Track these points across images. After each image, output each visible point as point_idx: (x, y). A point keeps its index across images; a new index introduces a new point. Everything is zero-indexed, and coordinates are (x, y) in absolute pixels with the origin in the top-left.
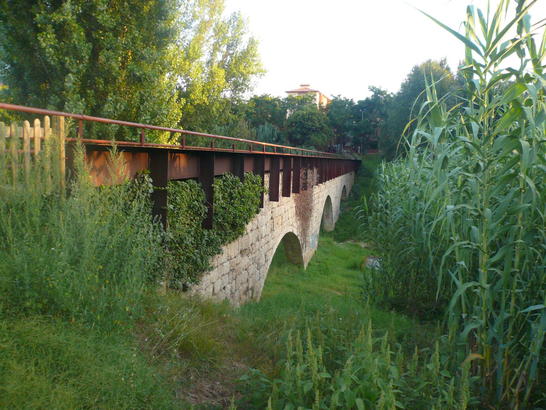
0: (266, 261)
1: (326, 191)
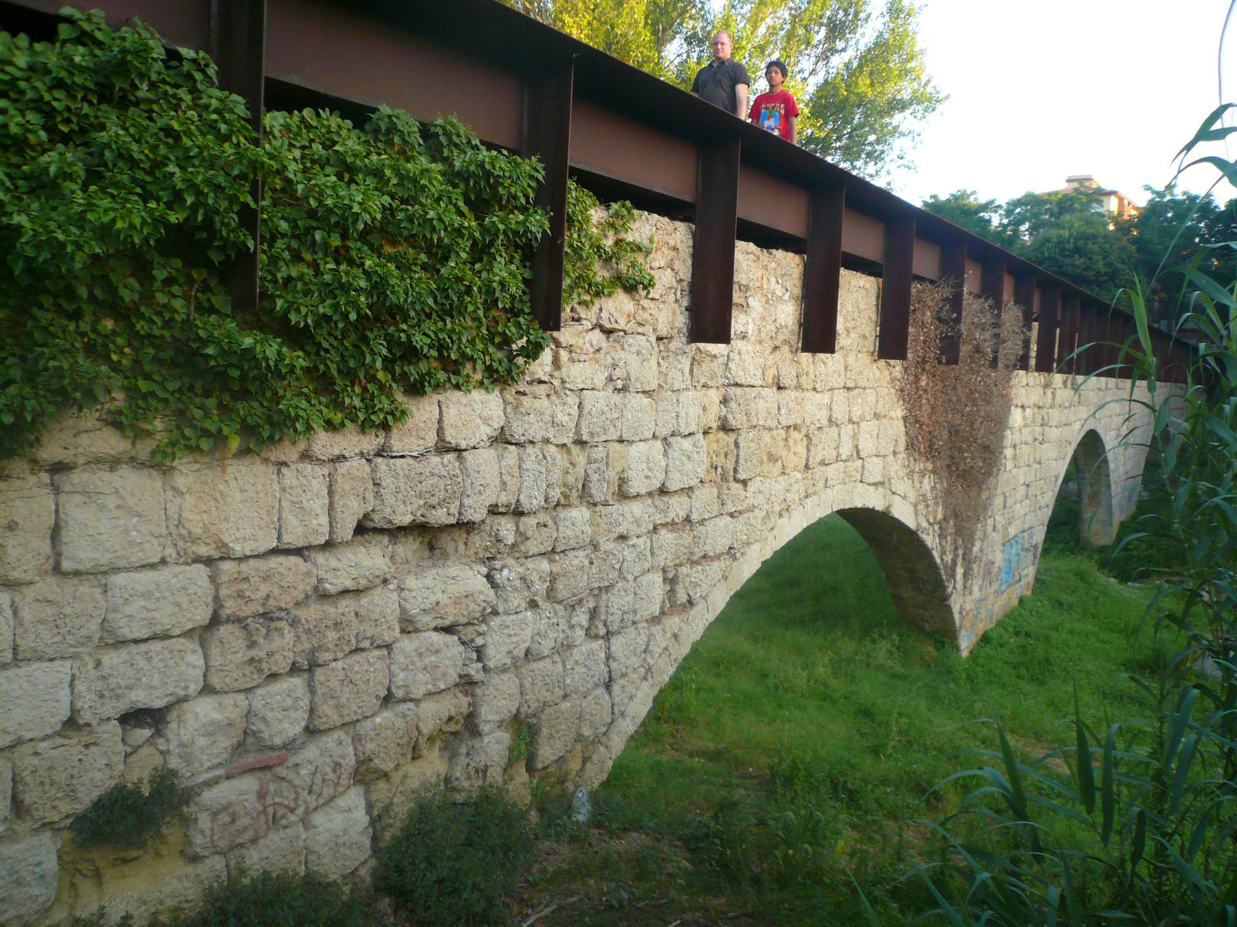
0: (676, 604)
1: (1084, 412)
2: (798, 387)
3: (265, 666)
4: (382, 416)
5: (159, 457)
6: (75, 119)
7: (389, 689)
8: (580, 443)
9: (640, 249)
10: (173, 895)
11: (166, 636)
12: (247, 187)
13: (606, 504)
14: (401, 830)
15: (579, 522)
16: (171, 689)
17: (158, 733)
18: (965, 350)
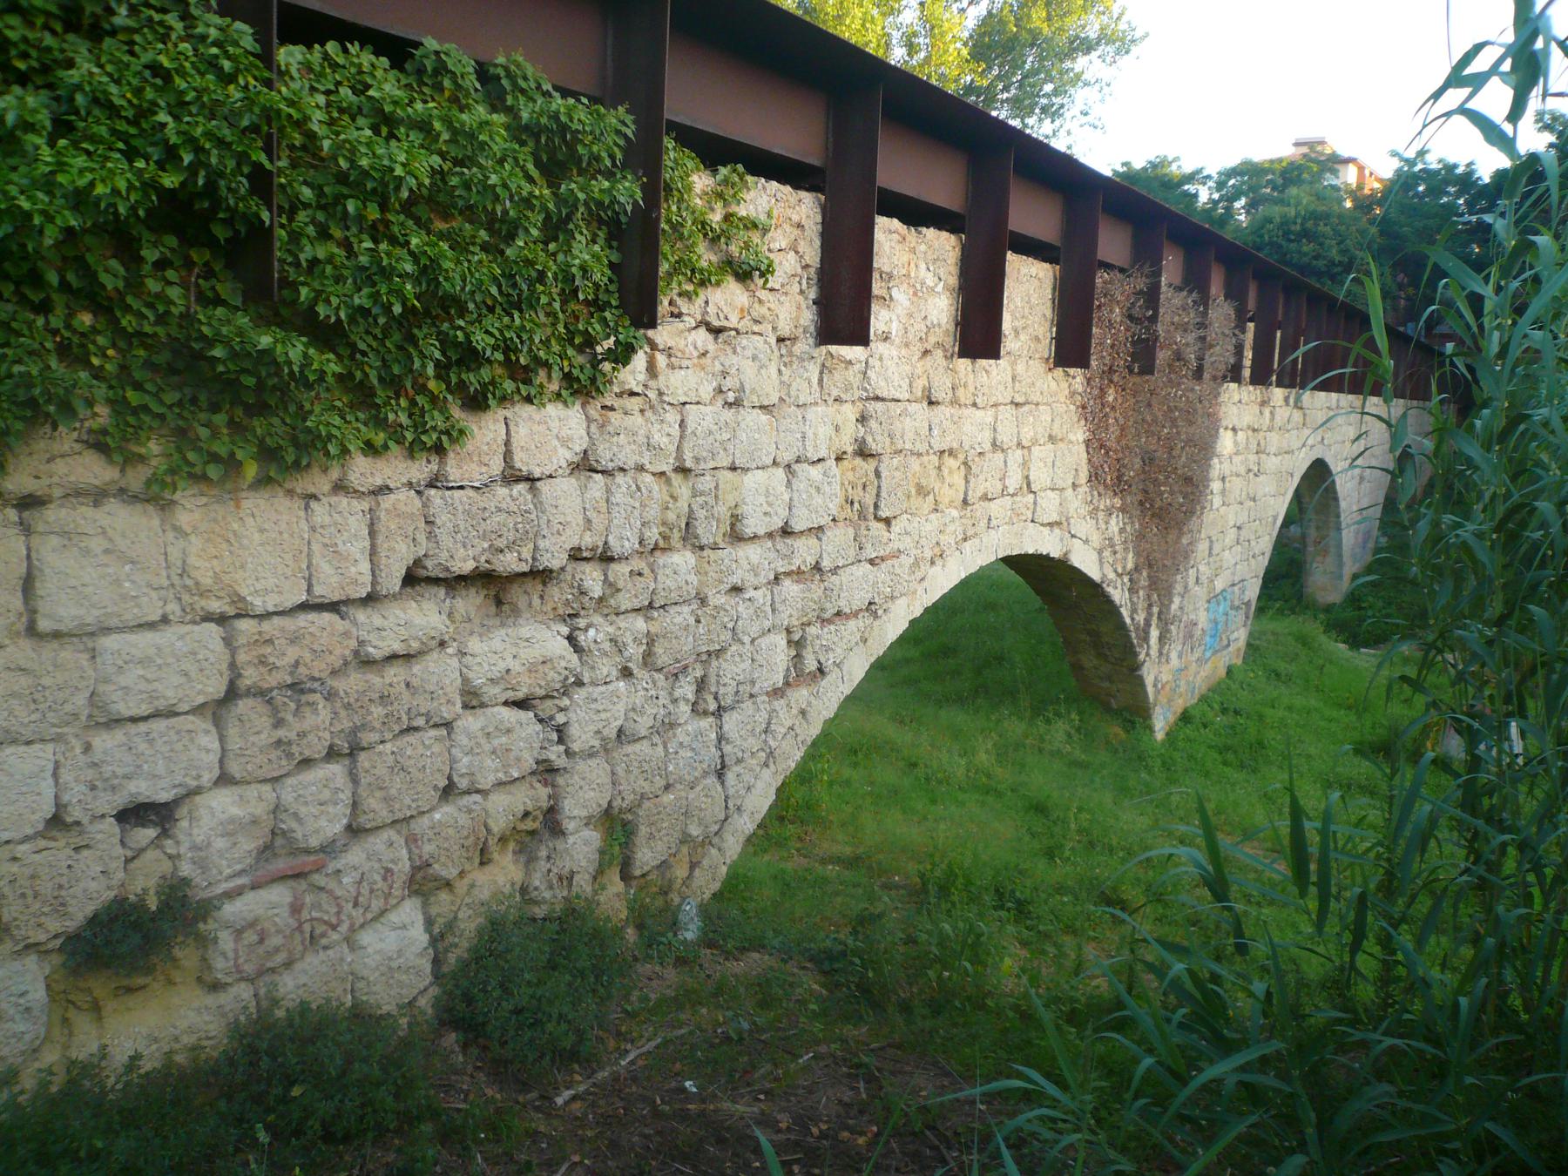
0: (805, 673)
2: (955, 402)
3: (295, 749)
4: (435, 436)
5: (155, 488)
6: (34, 53)
7: (449, 778)
8: (683, 470)
9: (755, 226)
10: (190, 1030)
11: (171, 713)
12: (260, 144)
13: (715, 547)
14: (469, 950)
15: (683, 569)
16: (179, 779)
17: (165, 833)
18: (1162, 356)
